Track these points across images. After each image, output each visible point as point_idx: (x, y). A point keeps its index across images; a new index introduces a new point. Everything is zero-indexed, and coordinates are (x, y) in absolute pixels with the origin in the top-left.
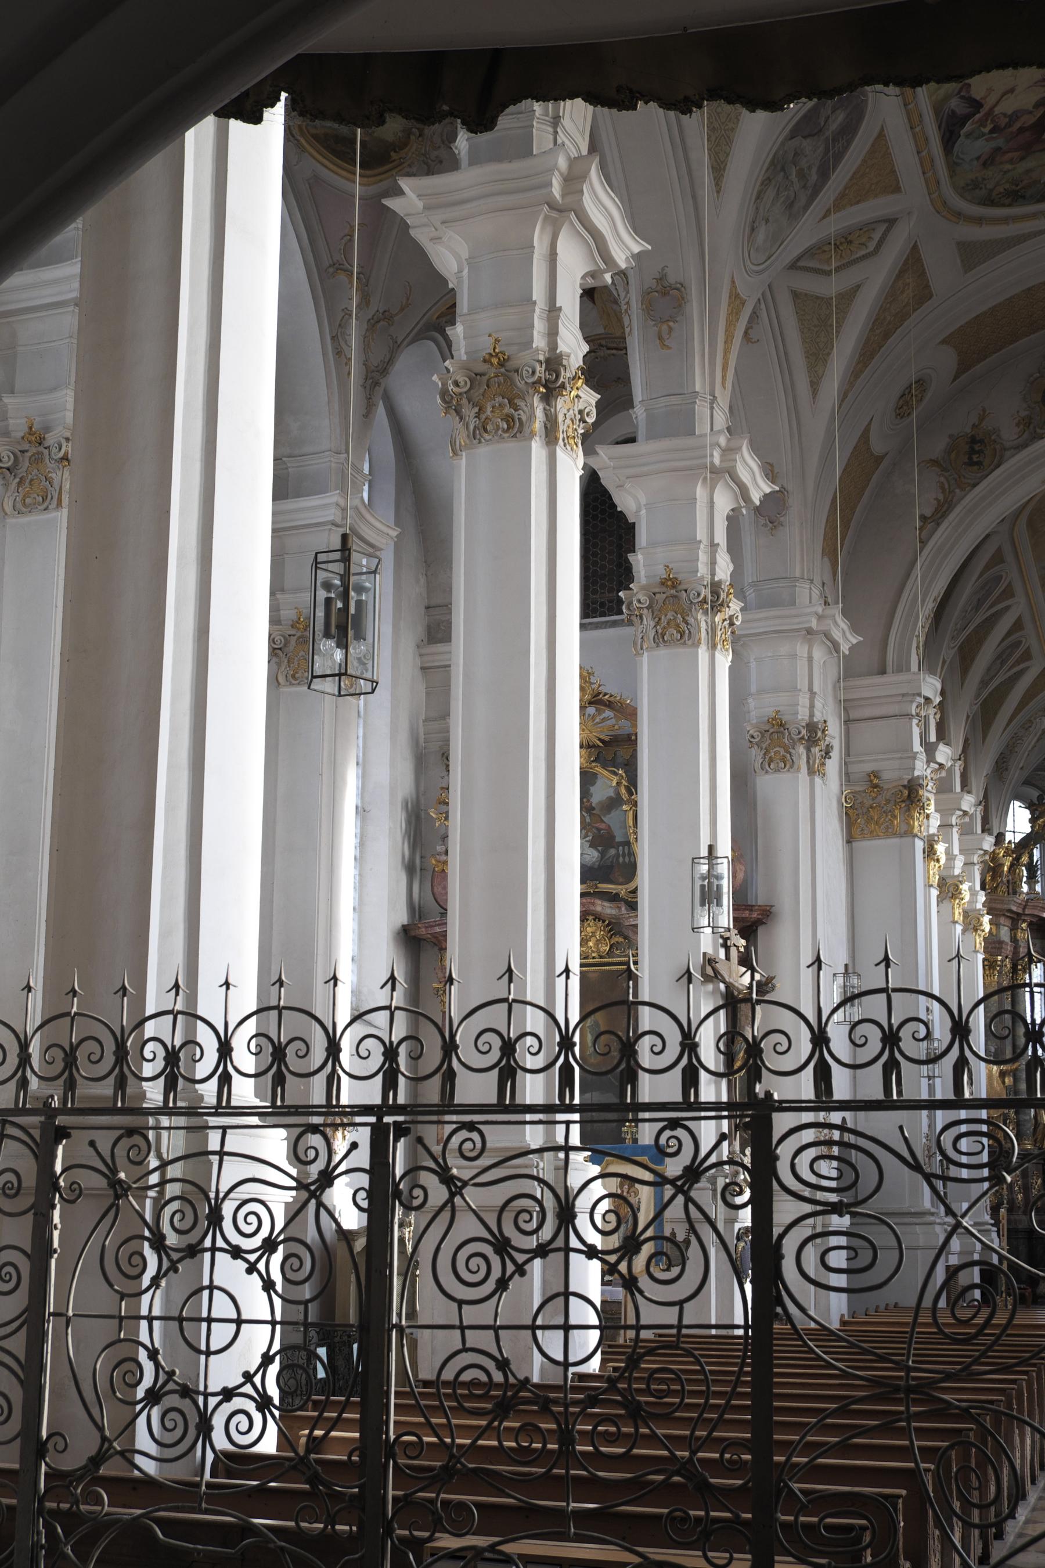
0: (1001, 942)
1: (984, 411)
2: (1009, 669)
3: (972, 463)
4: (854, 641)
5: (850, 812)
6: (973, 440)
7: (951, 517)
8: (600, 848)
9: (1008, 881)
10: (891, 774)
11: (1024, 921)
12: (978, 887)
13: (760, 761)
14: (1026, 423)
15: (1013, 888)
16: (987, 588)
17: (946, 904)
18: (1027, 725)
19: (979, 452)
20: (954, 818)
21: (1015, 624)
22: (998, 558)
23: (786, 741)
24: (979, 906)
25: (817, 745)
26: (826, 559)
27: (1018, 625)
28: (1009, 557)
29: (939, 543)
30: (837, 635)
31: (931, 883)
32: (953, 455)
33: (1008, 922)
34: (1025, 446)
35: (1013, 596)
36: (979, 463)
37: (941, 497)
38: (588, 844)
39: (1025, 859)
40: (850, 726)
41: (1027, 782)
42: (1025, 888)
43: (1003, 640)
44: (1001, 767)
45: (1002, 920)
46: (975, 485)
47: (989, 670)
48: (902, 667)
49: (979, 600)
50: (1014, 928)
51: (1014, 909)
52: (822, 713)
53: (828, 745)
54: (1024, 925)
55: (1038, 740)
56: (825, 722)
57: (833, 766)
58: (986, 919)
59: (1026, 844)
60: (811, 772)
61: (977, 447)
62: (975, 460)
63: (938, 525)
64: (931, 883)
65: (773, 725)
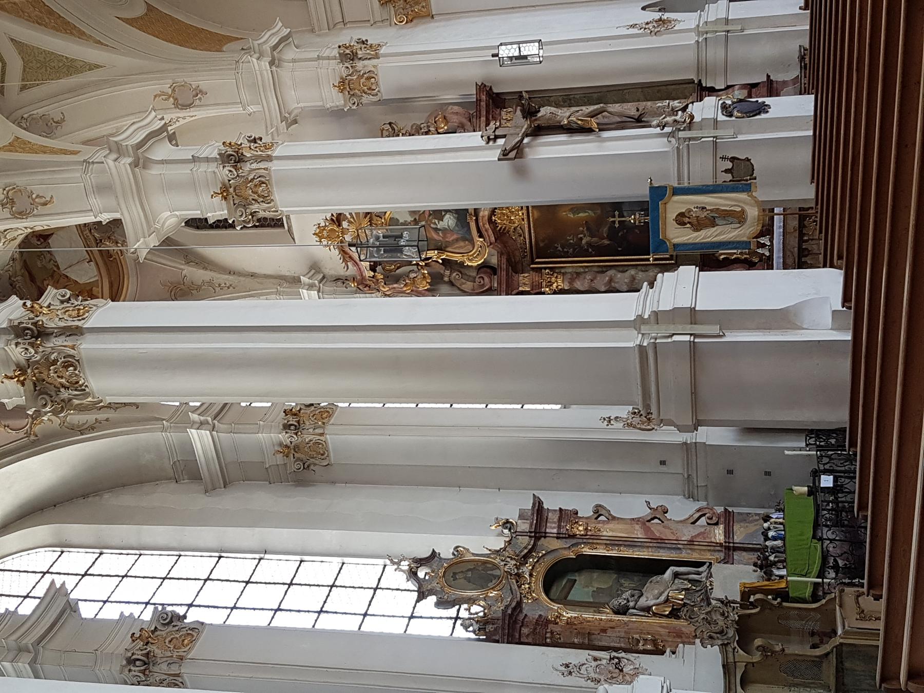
4: (280, 24)
5: (410, 17)
13: (371, 97)
23: (355, 77)
25: (356, 53)
30: (275, 40)
40: (347, 21)
52: (334, 48)
53: (358, 43)
56: (339, 47)
60: (377, 56)
65: (344, 88)
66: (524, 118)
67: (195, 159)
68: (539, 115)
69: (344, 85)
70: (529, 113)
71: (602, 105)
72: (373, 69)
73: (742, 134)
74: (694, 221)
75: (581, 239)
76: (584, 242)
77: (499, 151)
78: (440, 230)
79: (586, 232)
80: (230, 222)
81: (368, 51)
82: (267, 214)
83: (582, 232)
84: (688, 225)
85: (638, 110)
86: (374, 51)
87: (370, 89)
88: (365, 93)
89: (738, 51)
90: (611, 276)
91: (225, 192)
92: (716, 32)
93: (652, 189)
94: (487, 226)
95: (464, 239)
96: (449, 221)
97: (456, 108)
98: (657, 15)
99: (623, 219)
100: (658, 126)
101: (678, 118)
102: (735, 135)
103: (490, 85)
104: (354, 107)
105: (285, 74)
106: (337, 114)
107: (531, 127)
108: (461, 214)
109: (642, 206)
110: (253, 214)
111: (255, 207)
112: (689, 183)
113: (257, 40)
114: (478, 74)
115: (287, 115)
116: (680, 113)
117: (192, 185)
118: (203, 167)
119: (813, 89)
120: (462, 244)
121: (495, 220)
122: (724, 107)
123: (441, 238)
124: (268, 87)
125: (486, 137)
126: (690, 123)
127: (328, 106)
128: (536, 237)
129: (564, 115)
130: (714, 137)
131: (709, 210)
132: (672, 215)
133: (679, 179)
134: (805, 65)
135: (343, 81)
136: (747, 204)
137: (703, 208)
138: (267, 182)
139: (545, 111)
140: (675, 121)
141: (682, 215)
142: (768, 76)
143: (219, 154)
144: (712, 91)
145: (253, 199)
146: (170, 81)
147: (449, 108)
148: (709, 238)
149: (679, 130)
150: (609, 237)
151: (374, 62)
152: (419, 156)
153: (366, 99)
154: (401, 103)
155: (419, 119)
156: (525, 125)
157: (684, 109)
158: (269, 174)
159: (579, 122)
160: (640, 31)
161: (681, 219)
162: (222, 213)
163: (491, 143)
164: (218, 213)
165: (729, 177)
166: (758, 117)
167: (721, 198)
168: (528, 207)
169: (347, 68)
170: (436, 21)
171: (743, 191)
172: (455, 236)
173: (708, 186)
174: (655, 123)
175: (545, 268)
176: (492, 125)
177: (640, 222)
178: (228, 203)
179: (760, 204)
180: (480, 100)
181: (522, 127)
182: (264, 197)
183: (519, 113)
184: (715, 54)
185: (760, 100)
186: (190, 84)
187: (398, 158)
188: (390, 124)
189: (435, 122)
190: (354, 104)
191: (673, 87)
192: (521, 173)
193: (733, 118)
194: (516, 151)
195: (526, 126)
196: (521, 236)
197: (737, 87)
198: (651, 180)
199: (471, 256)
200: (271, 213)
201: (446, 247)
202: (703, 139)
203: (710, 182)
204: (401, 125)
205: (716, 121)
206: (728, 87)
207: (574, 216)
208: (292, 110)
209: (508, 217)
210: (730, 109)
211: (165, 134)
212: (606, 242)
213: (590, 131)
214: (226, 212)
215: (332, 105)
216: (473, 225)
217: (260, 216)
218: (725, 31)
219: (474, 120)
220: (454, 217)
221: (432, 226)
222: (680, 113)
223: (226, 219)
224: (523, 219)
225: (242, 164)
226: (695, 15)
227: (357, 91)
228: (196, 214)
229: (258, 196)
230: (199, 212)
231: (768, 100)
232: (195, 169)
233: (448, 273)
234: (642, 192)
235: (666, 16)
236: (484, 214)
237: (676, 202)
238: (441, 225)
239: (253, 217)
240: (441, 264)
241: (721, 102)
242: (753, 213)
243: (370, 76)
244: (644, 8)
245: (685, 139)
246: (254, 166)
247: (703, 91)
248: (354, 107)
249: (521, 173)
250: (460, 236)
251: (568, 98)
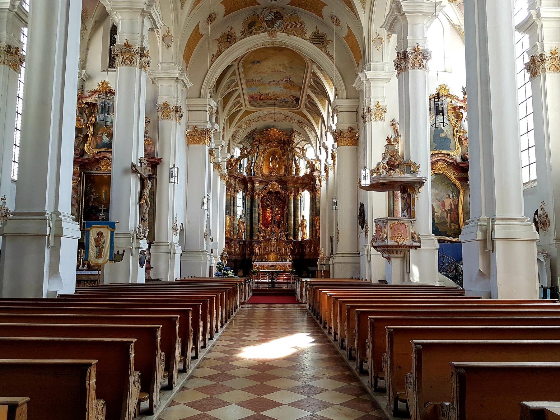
0: (232, 184)
1: (232, 27)
2: (236, 109)
3: (228, 41)
4: (191, 85)
6: (228, 35)
7: (221, 55)
8: (109, 138)
9: (234, 168)
10: (200, 126)
11: (238, 179)
12: (226, 168)
14: (243, 32)
15: (235, 170)
16: (231, 82)
17: (216, 170)
18: (241, 127)
19: (229, 39)
20: (220, 146)
21: (238, 95)
22: (234, 74)
24: (226, 173)
25: (178, 113)
26: (184, 61)
27: (239, 96)
28: (237, 74)
29: (217, 62)
30: (185, 82)
31: (211, 162)
32: (223, 38)
33: (233, 179)
34: (242, 39)
35: (238, 86)
36: (230, 42)
37: (219, 50)
38: (106, 136)
39: (239, 162)
41: (240, 143)
42: (238, 171)
43: (235, 99)
44: (234, 137)
45: (232, 178)
46: (228, 48)
47: (231, 108)
48: (205, 97)
49: (229, 85)
50: (235, 181)
51: (235, 175)
54: (237, 180)
55: (243, 131)
57: (183, 120)
58: (227, 177)
59: (239, 158)
60: (176, 121)
61: (229, 37)
62: (229, 41)
63: (217, 57)
64: (211, 162)
66: (148, 175)
67: (143, 36)
68: (148, 181)
69: (166, 106)
70: (150, 177)
71: (150, 206)
72: (171, 118)
73: (133, 257)
74: (99, 239)
75: (93, 194)
76: (92, 195)
77: (136, 164)
78: (102, 135)
79: (96, 196)
80: (115, 44)
81: (178, 118)
82: (117, 61)
83: (96, 195)
84: (97, 236)
85: (146, 219)
86: (178, 120)
87: (164, 116)
88: (162, 114)
89: (163, 257)
90: (75, 206)
91: (128, 46)
92: (171, 249)
93: (115, 223)
94: (102, 156)
95: (97, 145)
96: (106, 140)
97: (153, 149)
98: (179, 228)
99: (102, 211)
100: (139, 227)
101: (142, 234)
102: (132, 255)
103: (161, 164)
104: (157, 108)
105: (172, 83)
106: (155, 101)
107: (144, 177)
108: (110, 145)
109: (107, 218)
110: (117, 55)
111: (120, 57)
112: (115, 238)
113: (186, 74)
114: (165, 160)
115: (156, 80)
116: (144, 235)
117: (132, 33)
118: (139, 39)
119: (147, 283)
120: (95, 144)
121: (104, 159)
122: (144, 251)
123: (98, 135)
124: (168, 74)
125: (142, 159)
126: (139, 238)
127: (158, 98)
128: (95, 175)
129: (147, 191)
130: (133, 247)
131: (103, 245)
132: (102, 230)
133: (117, 234)
134: (156, 281)
135: (168, 106)
136: (104, 259)
137: (104, 243)
138: (131, 65)
139: (150, 184)
140: (141, 233)
141: (102, 234)
142: (152, 268)
143: (144, 47)
144: (149, 247)
145: (124, 57)
146: (174, 36)
147: (153, 147)
148: (91, 245)
149: (137, 234)
150: (92, 206)
151: (174, 119)
152: (136, 131)
153: (160, 114)
154: (157, 128)
155: (150, 134)
156: (145, 175)
157: (145, 237)
158: (134, 66)
159: (144, 196)
160: (174, 222)
161: (100, 234)
162: (119, 42)
163: (139, 161)
164: (119, 40)
165: (116, 253)
166: (139, 263)
167: (108, 249)
168: (111, 173)
169: (173, 108)
170: (186, 147)
171: (110, 258)
172: (99, 141)
173: (113, 244)
174: (141, 225)
175: (81, 178)
176: (146, 162)
177: (101, 217)
178: (123, 46)
179: (104, 264)
180: (155, 159)
181: (144, 174)
182: (125, 62)
183: (150, 173)
184: (163, 249)
185: (145, 264)
186: (172, 43)
187: (137, 122)
188: (149, 122)
189: (148, 140)
190: (158, 108)
191: (152, 233)
192: (126, 172)
193: (139, 255)
194: (135, 170)
195: (144, 175)
196: (96, 169)
197: (149, 257)
198: (118, 223)
199: (89, 147)
200: (117, 63)
201: (94, 137)
202: (132, 243)
203: (115, 245)
204: (148, 126)
205: (139, 248)
206: (150, 254)
207: (104, 192)
208: (158, 83)
209: (105, 165)
210: (143, 253)
211: (154, 27)
212: (90, 205)
213: (140, 200)
214: (119, 44)
215: (159, 99)
216: (103, 150)
217: (116, 58)
218: (171, 253)
219: (148, 156)
220: (107, 142)
221: (104, 132)
222: (144, 235)
223: (116, 43)
224: (104, 171)
225: (139, 56)
226: (177, 242)
227: (163, 110)
228: (119, 31)
229: (125, 60)
230: (120, 32)
231: (144, 267)
232: (139, 35)
233: (82, 136)
234: (112, 219)
235: (178, 231)
236: (108, 155)
237: (108, 232)
238: (104, 136)
239: (116, 55)
240: (86, 134)
241: (146, 250)
242: (100, 261)
243: (169, 117)
244: (182, 224)
245: (133, 236)
246: (138, 61)
247: (150, 244)
248: (157, 108)
249: (125, 172)
250: (99, 143)
251: (153, 194)
